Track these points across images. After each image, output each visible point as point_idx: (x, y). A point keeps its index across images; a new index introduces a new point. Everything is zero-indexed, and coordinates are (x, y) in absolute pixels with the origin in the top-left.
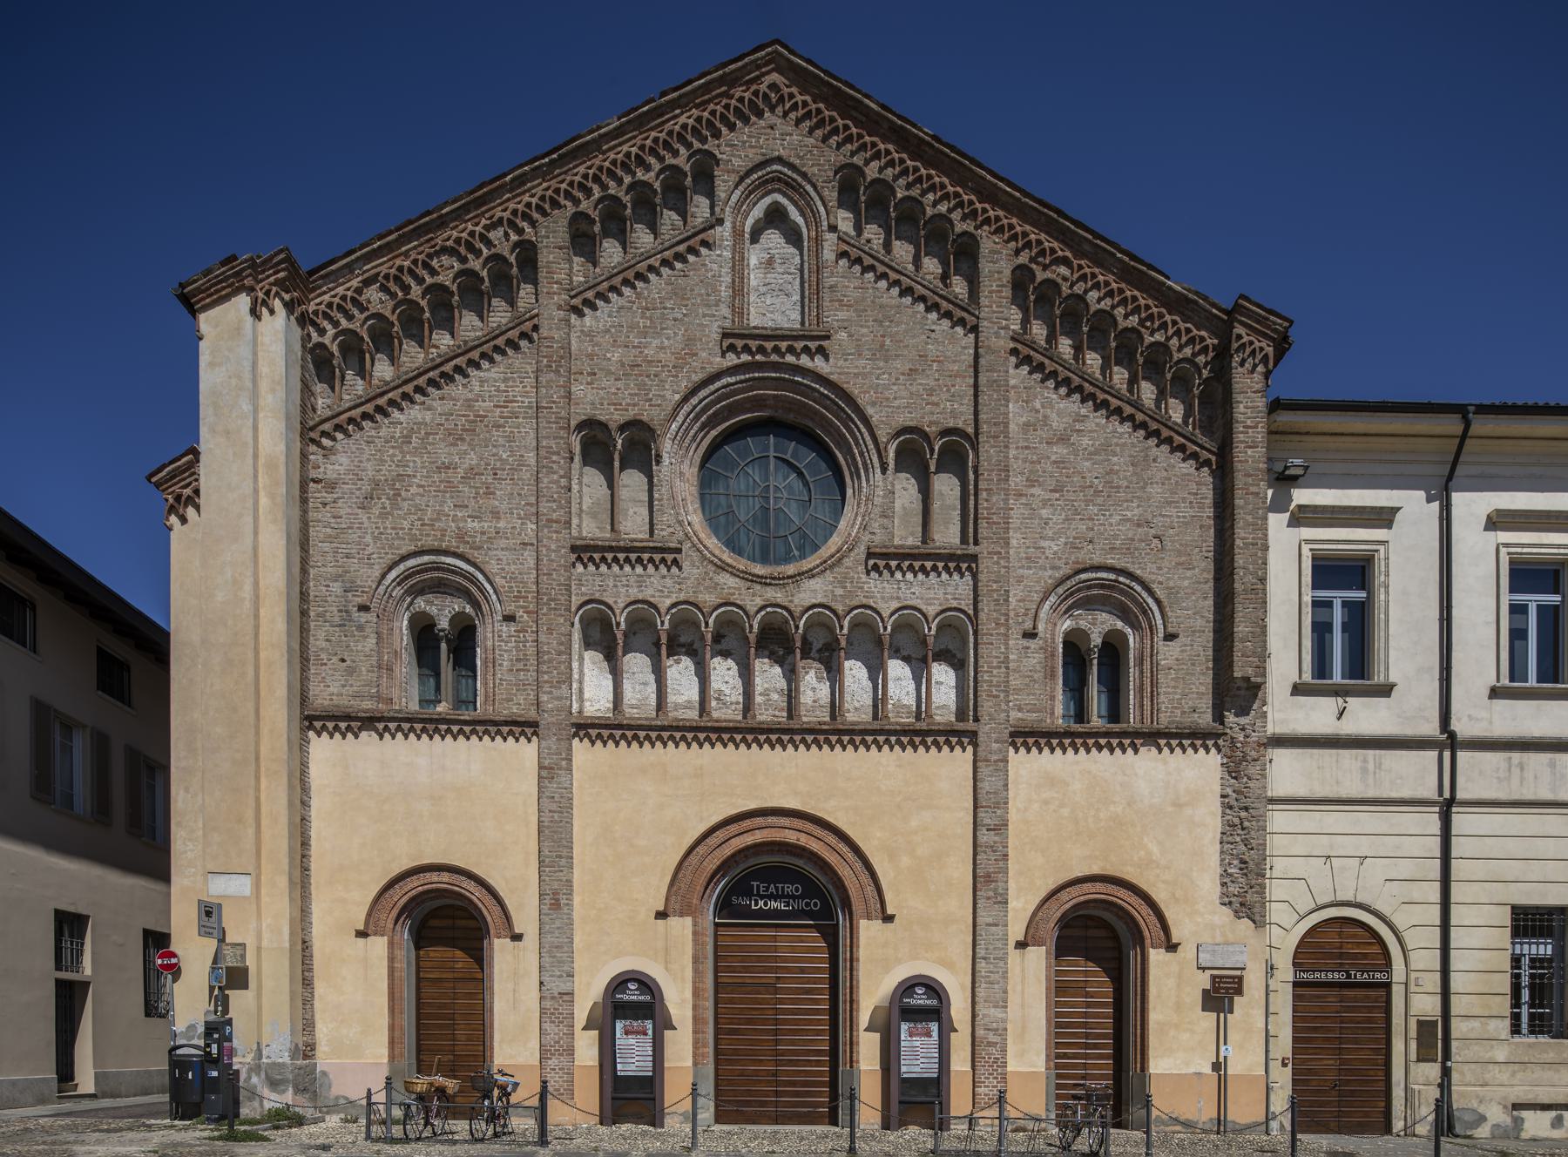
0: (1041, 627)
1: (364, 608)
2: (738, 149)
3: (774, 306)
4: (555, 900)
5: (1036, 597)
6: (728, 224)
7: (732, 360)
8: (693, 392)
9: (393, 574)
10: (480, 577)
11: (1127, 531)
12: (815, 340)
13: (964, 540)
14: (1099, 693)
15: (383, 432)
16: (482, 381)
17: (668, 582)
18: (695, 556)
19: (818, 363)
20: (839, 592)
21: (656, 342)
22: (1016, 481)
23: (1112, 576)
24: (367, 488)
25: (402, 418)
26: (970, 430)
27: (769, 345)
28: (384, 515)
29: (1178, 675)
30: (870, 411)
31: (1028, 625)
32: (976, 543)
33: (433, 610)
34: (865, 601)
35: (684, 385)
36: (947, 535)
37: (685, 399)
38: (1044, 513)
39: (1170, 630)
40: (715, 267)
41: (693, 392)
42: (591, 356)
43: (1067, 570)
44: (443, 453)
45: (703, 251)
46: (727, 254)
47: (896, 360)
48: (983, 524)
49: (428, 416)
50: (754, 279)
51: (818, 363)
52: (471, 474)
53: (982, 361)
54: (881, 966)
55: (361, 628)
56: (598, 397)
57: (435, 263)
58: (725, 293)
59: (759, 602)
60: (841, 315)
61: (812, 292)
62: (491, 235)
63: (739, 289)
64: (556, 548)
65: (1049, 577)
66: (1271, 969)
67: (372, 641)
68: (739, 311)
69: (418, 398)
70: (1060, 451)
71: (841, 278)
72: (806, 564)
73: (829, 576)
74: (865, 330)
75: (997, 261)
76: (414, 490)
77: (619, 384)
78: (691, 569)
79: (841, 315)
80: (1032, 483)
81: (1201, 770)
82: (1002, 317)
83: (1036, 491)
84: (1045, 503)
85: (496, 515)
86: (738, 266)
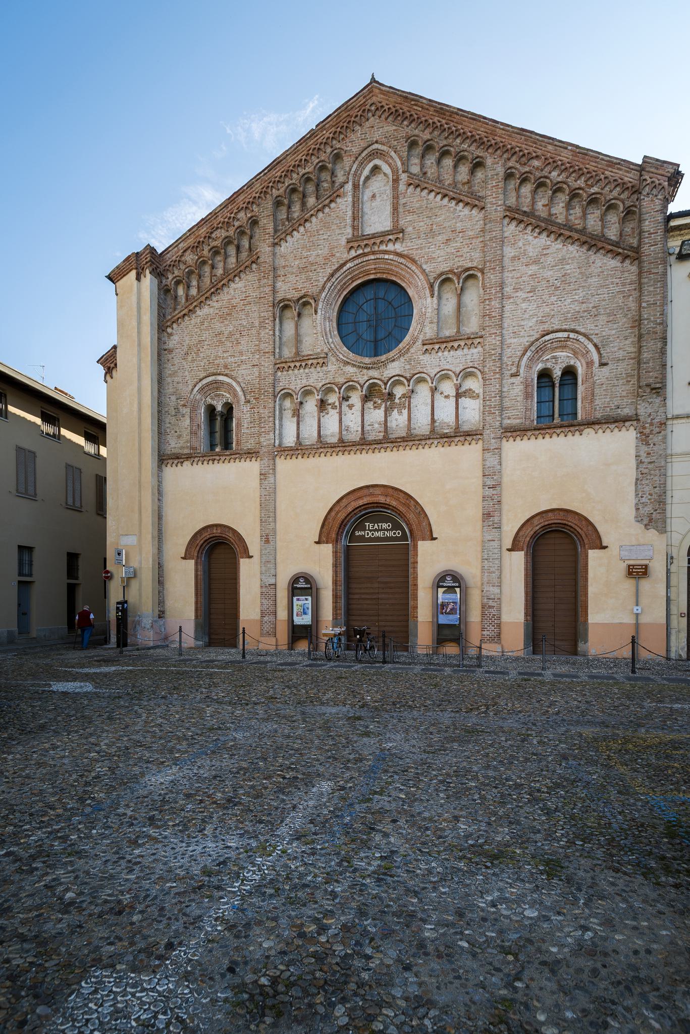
0: (522, 370)
1: (184, 405)
4: (267, 539)
5: (519, 354)
7: (353, 253)
8: (332, 275)
9: (197, 388)
11: (576, 307)
14: (557, 401)
15: (193, 322)
17: (321, 374)
18: (334, 359)
19: (398, 247)
20: (408, 367)
21: (315, 253)
23: (565, 334)
24: (185, 348)
25: (201, 314)
28: (193, 361)
29: (602, 386)
30: (424, 267)
31: (514, 370)
33: (214, 403)
34: (421, 370)
37: (329, 280)
38: (524, 306)
39: (604, 361)
40: (344, 207)
41: (332, 275)
43: (537, 336)
44: (218, 326)
46: (350, 199)
49: (212, 310)
51: (398, 247)
52: (231, 334)
54: (429, 560)
55: (183, 416)
56: (287, 289)
58: (349, 221)
59: (366, 378)
65: (525, 341)
66: (670, 559)
67: (188, 422)
70: (534, 268)
72: (391, 354)
73: (402, 359)
74: (422, 224)
77: (298, 278)
78: (332, 367)
79: (409, 218)
80: (516, 290)
81: (624, 441)
83: (519, 294)
84: (524, 300)
85: (241, 353)
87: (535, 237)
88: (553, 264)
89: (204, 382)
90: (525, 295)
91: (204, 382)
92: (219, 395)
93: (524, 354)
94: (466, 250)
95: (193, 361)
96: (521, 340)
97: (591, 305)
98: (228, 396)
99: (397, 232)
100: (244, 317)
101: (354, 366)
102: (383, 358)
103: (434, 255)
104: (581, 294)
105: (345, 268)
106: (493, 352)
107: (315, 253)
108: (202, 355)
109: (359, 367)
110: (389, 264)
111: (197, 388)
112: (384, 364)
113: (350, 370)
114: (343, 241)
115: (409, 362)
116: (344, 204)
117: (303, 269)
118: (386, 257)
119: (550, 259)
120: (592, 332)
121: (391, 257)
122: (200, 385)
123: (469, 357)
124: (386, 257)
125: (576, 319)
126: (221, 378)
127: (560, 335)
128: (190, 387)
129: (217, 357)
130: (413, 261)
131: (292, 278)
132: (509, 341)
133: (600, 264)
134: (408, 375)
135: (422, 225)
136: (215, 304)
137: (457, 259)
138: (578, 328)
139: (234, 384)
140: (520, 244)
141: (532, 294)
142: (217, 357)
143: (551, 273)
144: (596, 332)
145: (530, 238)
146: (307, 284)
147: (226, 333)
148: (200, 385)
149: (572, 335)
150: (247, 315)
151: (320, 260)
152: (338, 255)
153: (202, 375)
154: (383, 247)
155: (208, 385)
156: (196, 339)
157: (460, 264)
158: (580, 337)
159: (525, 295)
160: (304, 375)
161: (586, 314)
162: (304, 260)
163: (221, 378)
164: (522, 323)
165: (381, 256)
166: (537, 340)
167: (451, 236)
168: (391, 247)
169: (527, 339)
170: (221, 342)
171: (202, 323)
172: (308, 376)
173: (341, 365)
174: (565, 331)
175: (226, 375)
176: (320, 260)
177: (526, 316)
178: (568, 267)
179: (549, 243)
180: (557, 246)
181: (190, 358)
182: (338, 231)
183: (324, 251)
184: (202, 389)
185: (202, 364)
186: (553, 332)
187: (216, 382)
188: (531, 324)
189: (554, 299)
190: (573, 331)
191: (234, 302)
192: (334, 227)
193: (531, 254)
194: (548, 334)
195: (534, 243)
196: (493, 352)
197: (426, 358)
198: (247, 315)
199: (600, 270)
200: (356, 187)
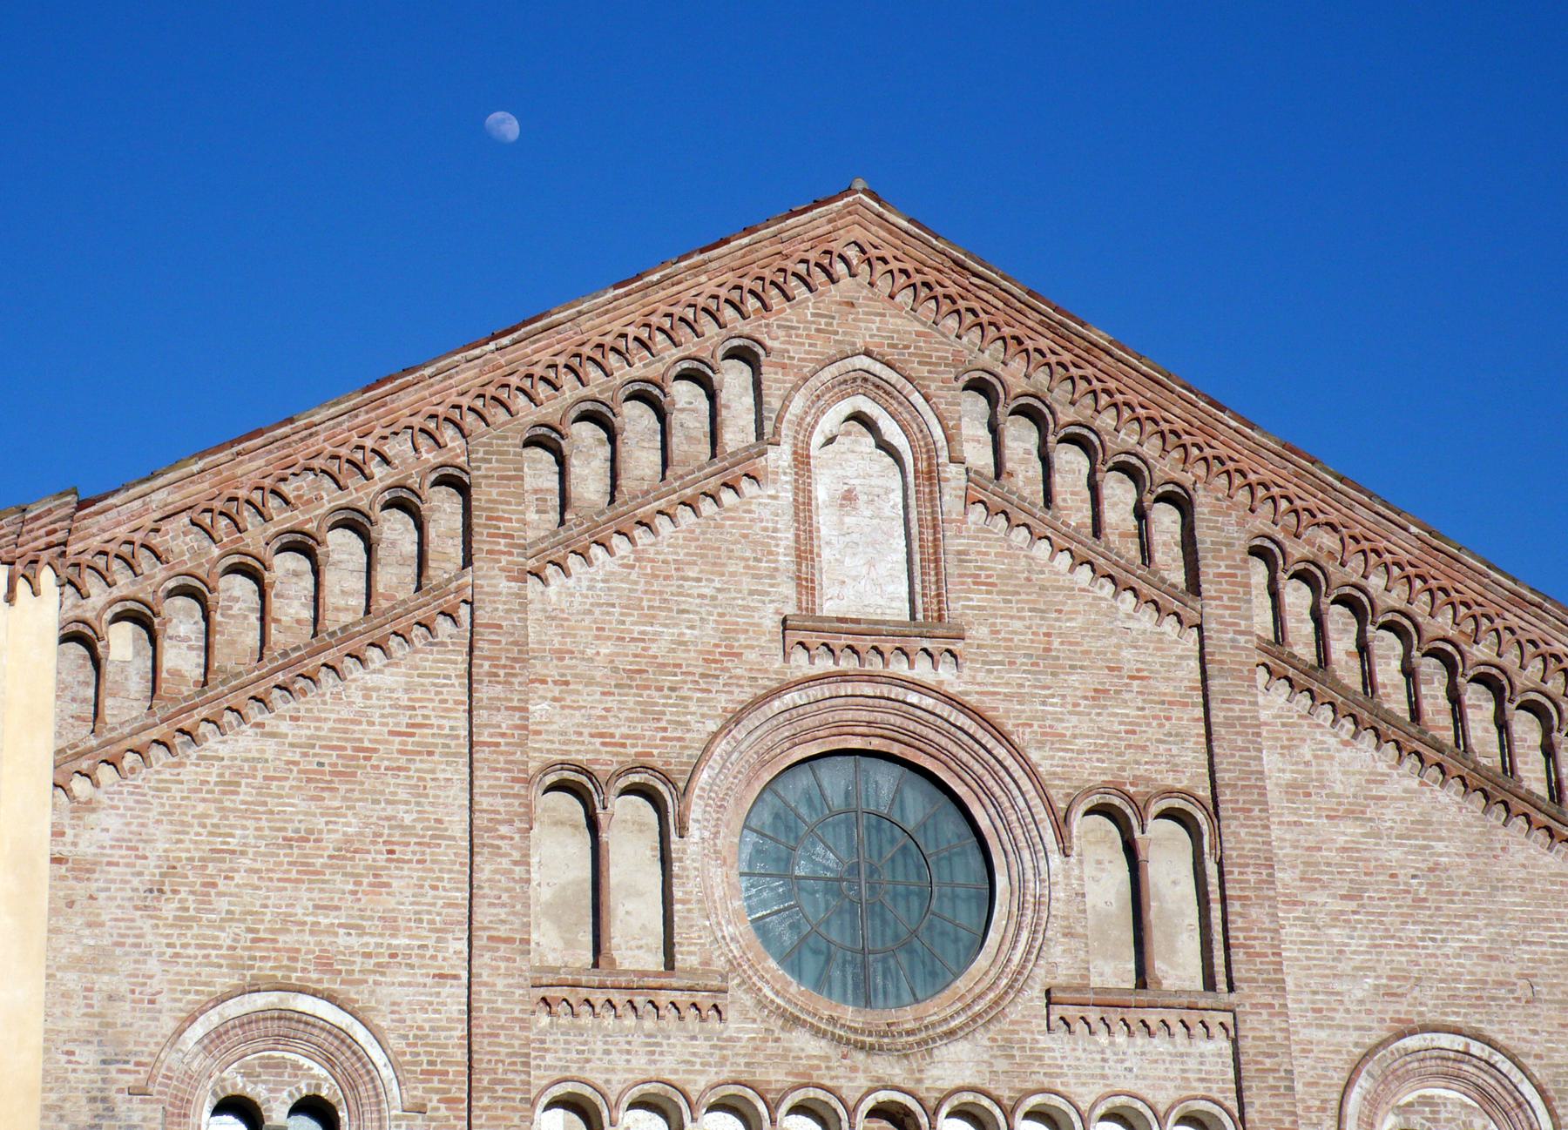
2: (791, 329)
3: (866, 578)
5: (1339, 1078)
6: (786, 448)
8: (737, 718)
9: (197, 1031)
10: (361, 1034)
11: (1471, 965)
12: (931, 627)
13: (1209, 983)
15: (189, 773)
16: (367, 692)
17: (702, 1046)
18: (748, 1000)
19: (946, 676)
20: (1002, 1065)
21: (669, 633)
22: (1285, 877)
23: (1458, 1043)
24: (151, 868)
25: (223, 750)
26: (1204, 793)
27: (863, 643)
28: (182, 921)
30: (1034, 756)
32: (1231, 988)
34: (1047, 1082)
35: (723, 702)
36: (1179, 965)
37: (725, 729)
38: (1336, 934)
40: (766, 514)
41: (737, 718)
42: (560, 654)
43: (1379, 1033)
44: (297, 808)
45: (745, 484)
47: (1074, 671)
48: (1238, 955)
49: (270, 746)
50: (825, 521)
51: (946, 676)
52: (347, 850)
53: (1215, 684)
56: (564, 726)
57: (285, 488)
58: (785, 560)
59: (863, 1082)
60: (977, 599)
61: (926, 555)
62: (389, 449)
63: (805, 551)
64: (503, 988)
65: (1351, 1042)
68: (806, 585)
69: (254, 712)
70: (1349, 831)
71: (969, 532)
73: (982, 1038)
74: (1017, 625)
75: (1226, 525)
76: (239, 878)
77: (610, 702)
78: (741, 1025)
79: (977, 599)
80: (1311, 881)
82: (1242, 606)
83: (1320, 897)
84: (1336, 918)
85: (390, 924)
86: (803, 506)
87: (1346, 744)
88: (1400, 828)
89: (233, 1008)
90: (1337, 905)
91: (233, 1008)
92: (280, 1065)
93: (1349, 1084)
94: (1153, 732)
95: (182, 921)
96: (1339, 1036)
97: (1514, 969)
98: (319, 1071)
99: (931, 627)
100: (403, 795)
101: (818, 1032)
102: (907, 1017)
103: (1060, 728)
104: (1481, 933)
105: (777, 705)
106: (1268, 1063)
107: (669, 633)
108: (223, 904)
109: (840, 1040)
110: (918, 720)
111: (197, 1031)
112: (925, 1042)
113: (806, 1045)
114: (771, 623)
115: (1006, 1047)
116: (768, 503)
117: (632, 678)
118: (913, 698)
119: (1389, 813)
120: (1525, 1047)
121: (928, 702)
122: (213, 1018)
123: (1192, 1064)
124: (913, 698)
125: (1478, 1002)
126: (305, 1004)
127: (1445, 1040)
128: (168, 1024)
129: (287, 922)
130: (1002, 736)
131: (589, 697)
132: (1306, 1034)
133: (1520, 858)
134: (1005, 1094)
135: (1021, 628)
136: (285, 727)
137: (1129, 755)
138: (1490, 1030)
139: (361, 1034)
140: (1306, 752)
141: (1353, 905)
142: (287, 922)
143: (1396, 854)
144: (1537, 1049)
145: (1332, 742)
146: (646, 729)
147: (331, 840)
148: (213, 1018)
149: (1476, 1048)
150: (419, 791)
151: (690, 659)
152: (751, 656)
153: (225, 981)
154: (900, 667)
155: (246, 1021)
156: (196, 842)
157: (1141, 770)
158: (1498, 1058)
159: (1337, 905)
160: (638, 1040)
161: (1503, 992)
162: (634, 648)
163: (305, 1004)
164: (1337, 987)
165: (896, 692)
166: (1384, 1043)
167: (1109, 682)
168: (922, 670)
169: (1354, 1036)
170: (307, 869)
171: (230, 787)
172: (652, 1048)
173: (776, 1023)
174: (1457, 1032)
175: (330, 998)
176: (690, 659)
177: (1342, 967)
178: (1439, 847)
179: (1382, 767)
180: (1407, 782)
181: (169, 910)
182: (747, 583)
183: (708, 635)
184: (217, 1036)
185: (225, 939)
186: (1425, 1029)
187: (283, 1015)
188: (1359, 994)
189: (1414, 930)
190: (1478, 1037)
191: (367, 734)
192: (734, 566)
193: (1338, 789)
194: (1412, 1033)
195: (1354, 761)
196: (1268, 1063)
197: (1057, 1046)
198: (419, 791)
199: (1522, 874)
200: (802, 460)
